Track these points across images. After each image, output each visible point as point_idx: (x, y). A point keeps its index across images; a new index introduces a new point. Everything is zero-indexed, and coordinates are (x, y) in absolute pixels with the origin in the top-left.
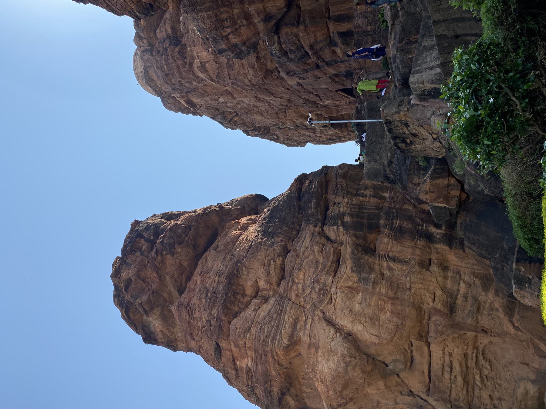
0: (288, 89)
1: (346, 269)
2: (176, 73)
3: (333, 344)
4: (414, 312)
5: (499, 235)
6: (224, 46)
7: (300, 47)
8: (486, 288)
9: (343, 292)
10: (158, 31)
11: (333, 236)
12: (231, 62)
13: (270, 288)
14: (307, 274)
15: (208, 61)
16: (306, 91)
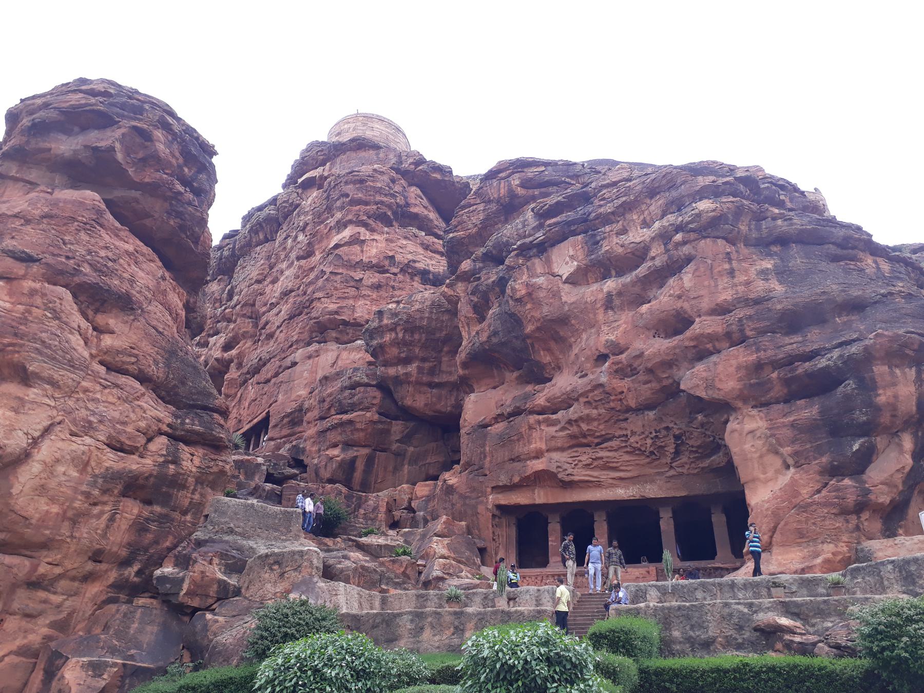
0: (291, 346)
1: (111, 460)
2: (360, 195)
3: (20, 433)
4: (43, 539)
5: (145, 646)
6: (385, 321)
7: (353, 408)
8: (52, 625)
9: (84, 453)
10: (419, 192)
11: (152, 447)
12: (352, 284)
13: (100, 351)
14: (112, 407)
15: (362, 251)
16: (281, 370)
